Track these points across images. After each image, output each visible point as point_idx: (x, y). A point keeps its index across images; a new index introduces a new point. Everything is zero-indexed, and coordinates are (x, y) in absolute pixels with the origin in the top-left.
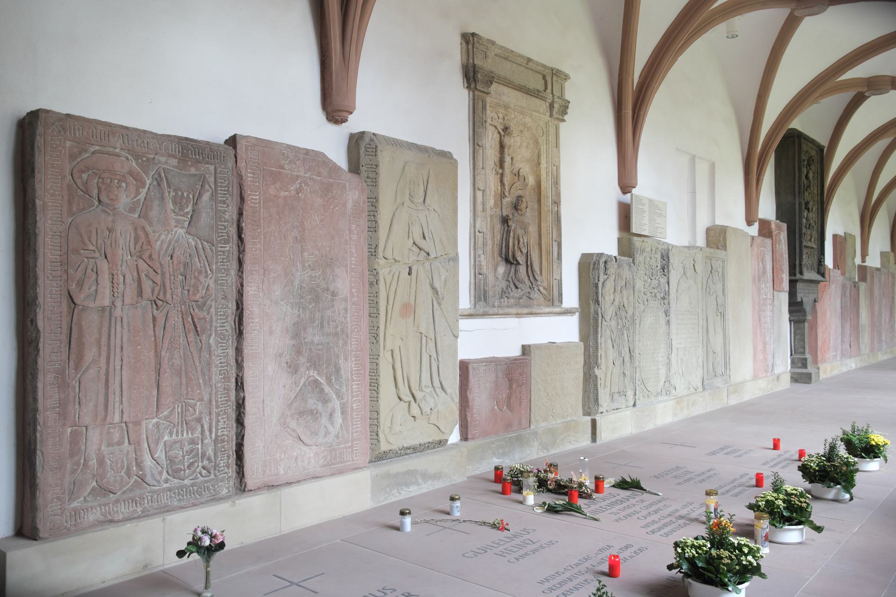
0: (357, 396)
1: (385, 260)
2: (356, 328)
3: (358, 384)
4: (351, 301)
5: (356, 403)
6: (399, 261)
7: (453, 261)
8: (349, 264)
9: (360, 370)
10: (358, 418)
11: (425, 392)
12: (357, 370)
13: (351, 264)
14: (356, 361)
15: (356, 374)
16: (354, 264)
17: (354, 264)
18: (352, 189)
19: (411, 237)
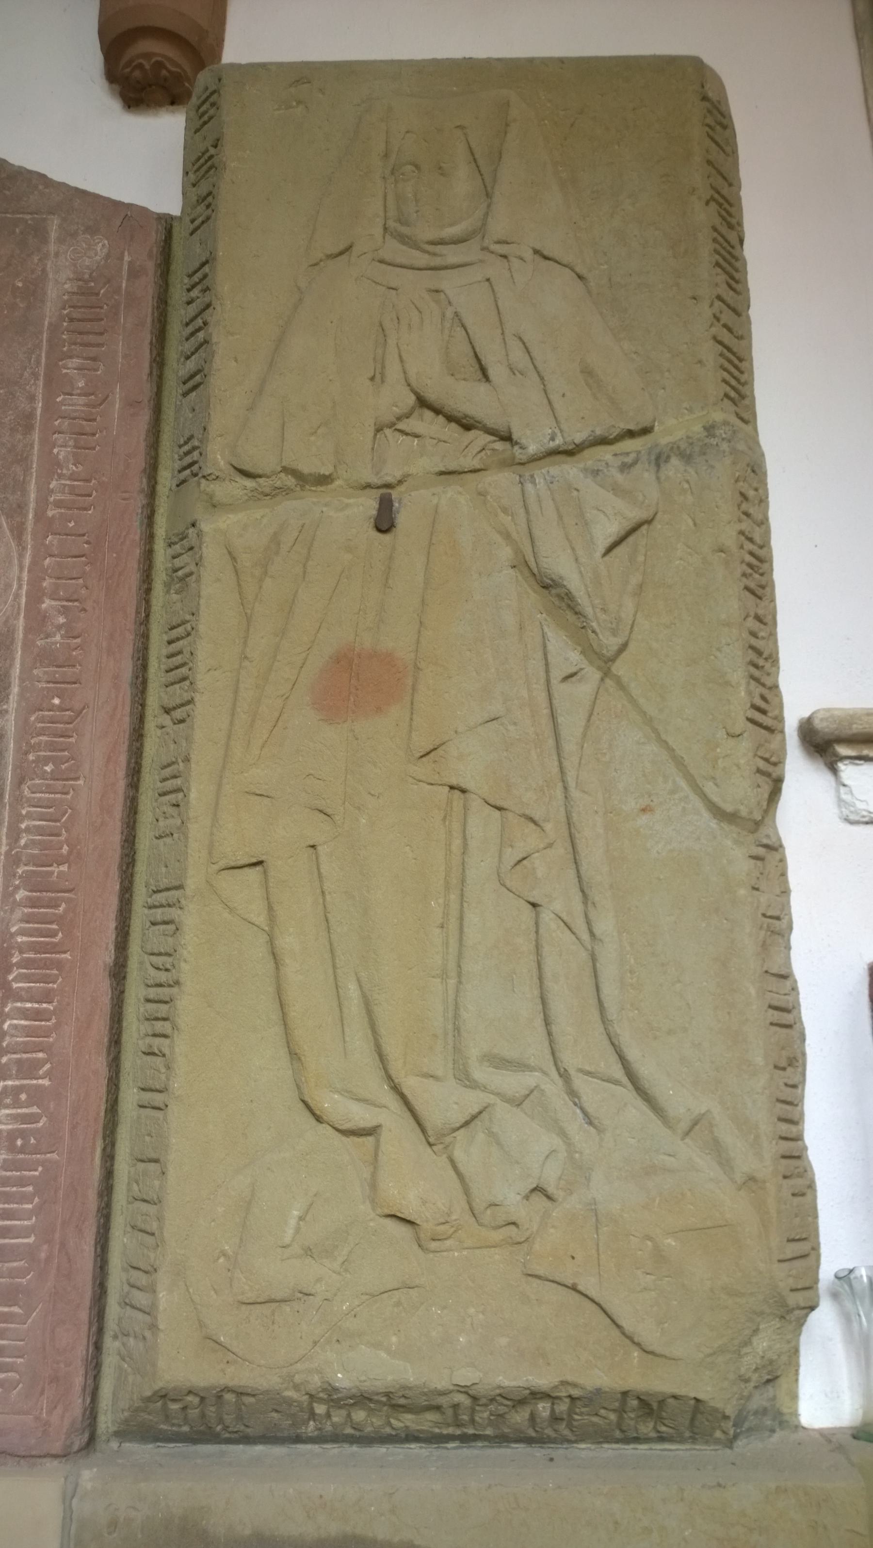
0: (28, 1069)
1: (249, 483)
2: (46, 760)
3: (37, 1015)
4: (27, 645)
5: (17, 1104)
6: (324, 480)
7: (687, 458)
8: (32, 505)
9: (54, 948)
10: (22, 1182)
11: (484, 1088)
12: (34, 947)
13: (42, 504)
14: (33, 903)
15: (27, 964)
16: (58, 504)
17: (58, 504)
18: (74, 235)
19: (393, 371)
